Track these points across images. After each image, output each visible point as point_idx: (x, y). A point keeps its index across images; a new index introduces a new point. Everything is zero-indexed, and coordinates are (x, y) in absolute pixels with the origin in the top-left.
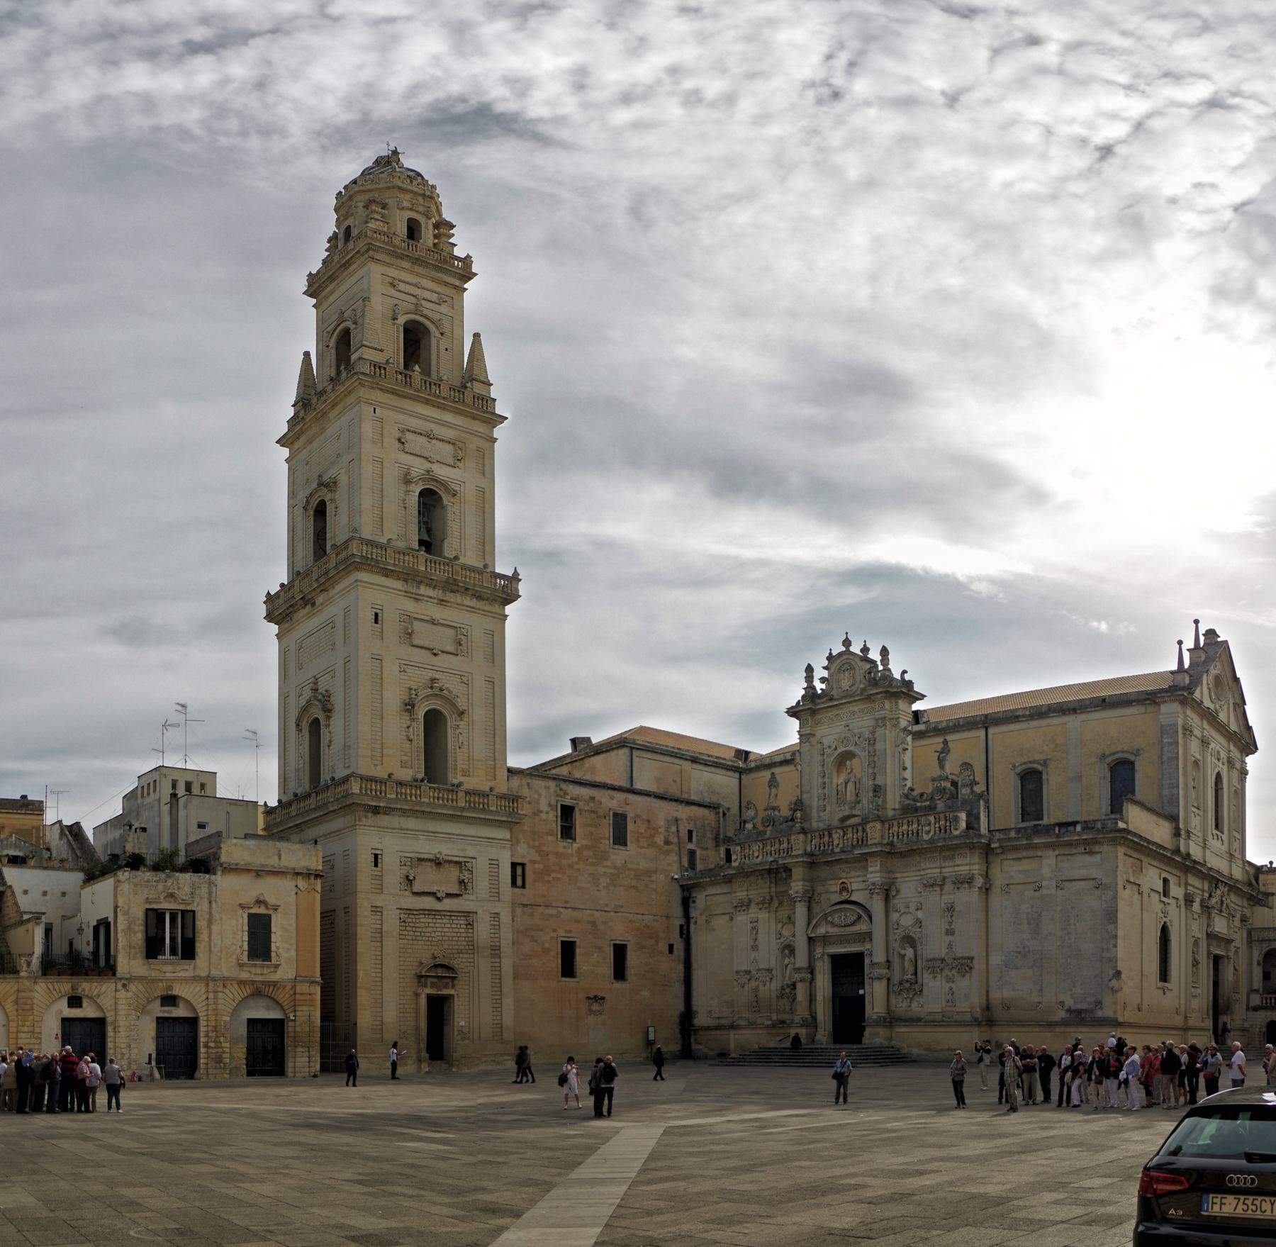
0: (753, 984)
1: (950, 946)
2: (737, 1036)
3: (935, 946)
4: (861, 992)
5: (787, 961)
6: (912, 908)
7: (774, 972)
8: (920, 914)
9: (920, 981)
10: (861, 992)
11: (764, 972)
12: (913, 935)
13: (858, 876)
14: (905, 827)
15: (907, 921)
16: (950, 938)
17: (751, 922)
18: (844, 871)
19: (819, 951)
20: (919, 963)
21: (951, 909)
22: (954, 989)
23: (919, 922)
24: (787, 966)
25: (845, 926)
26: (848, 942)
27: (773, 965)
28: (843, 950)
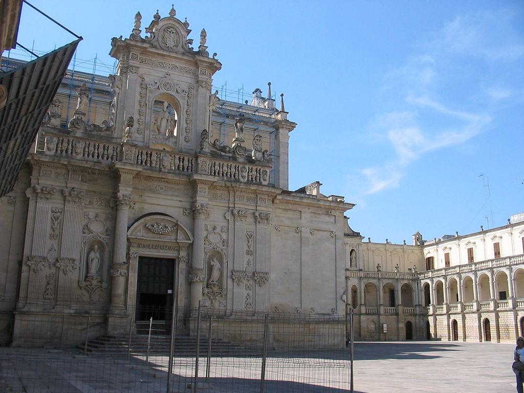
0: (46, 271)
1: (248, 263)
2: (23, 323)
3: (242, 262)
4: (170, 292)
5: (92, 255)
6: (218, 230)
7: (77, 263)
8: (224, 236)
9: (225, 287)
10: (170, 292)
11: (66, 261)
12: (220, 251)
13: (176, 196)
14: (225, 168)
15: (214, 239)
16: (251, 258)
17: (53, 212)
18: (162, 188)
19: (133, 250)
20: (225, 273)
21: (250, 236)
22: (251, 294)
23: (225, 243)
24: (92, 260)
25: (162, 234)
26: (162, 248)
27: (76, 256)
28: (156, 254)
